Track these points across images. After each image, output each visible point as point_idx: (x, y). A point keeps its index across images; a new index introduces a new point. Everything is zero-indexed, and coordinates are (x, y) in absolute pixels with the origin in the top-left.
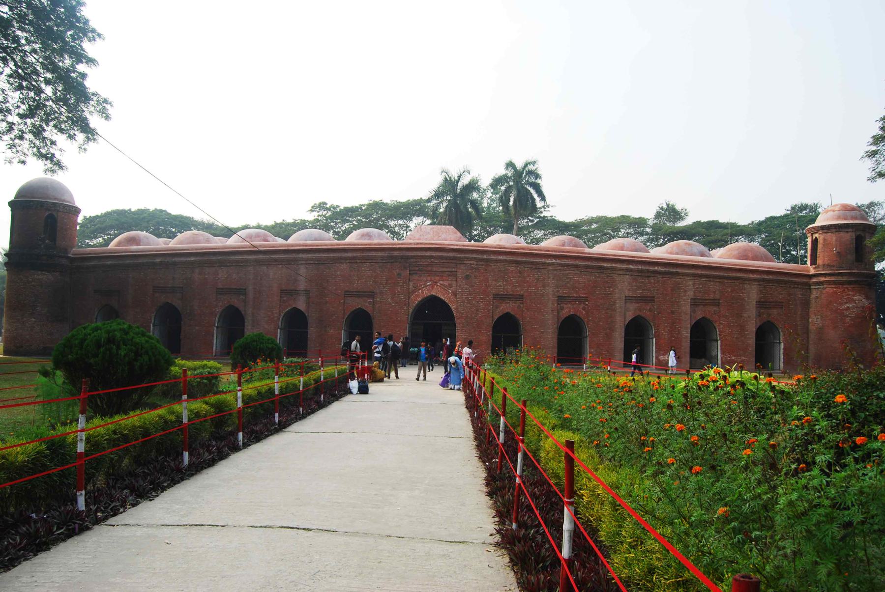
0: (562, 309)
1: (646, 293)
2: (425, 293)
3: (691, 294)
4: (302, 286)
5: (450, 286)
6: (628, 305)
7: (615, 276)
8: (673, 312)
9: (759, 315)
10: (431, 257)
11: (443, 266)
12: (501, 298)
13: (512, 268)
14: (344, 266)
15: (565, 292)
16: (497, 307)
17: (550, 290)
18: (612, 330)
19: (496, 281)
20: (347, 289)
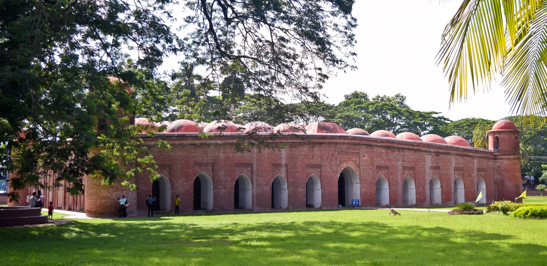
0: (404, 173)
1: (437, 165)
2: (344, 165)
3: (453, 164)
4: (284, 162)
5: (356, 161)
6: (430, 171)
7: (425, 155)
8: (447, 175)
9: (477, 175)
10: (348, 144)
11: (353, 149)
12: (379, 168)
13: (383, 151)
14: (306, 148)
15: (406, 164)
16: (377, 173)
17: (400, 163)
18: (425, 184)
19: (377, 158)
20: (307, 163)
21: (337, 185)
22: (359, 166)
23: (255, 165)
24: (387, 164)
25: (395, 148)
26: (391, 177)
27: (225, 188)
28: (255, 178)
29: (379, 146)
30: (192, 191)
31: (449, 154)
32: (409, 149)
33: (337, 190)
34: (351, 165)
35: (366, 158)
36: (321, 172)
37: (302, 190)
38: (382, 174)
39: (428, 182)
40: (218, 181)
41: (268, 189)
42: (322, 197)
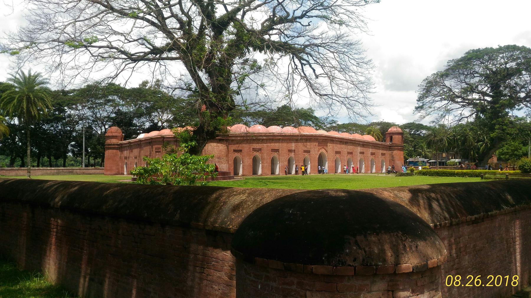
24: (340, 150)
34: (323, 151)
38: (338, 156)
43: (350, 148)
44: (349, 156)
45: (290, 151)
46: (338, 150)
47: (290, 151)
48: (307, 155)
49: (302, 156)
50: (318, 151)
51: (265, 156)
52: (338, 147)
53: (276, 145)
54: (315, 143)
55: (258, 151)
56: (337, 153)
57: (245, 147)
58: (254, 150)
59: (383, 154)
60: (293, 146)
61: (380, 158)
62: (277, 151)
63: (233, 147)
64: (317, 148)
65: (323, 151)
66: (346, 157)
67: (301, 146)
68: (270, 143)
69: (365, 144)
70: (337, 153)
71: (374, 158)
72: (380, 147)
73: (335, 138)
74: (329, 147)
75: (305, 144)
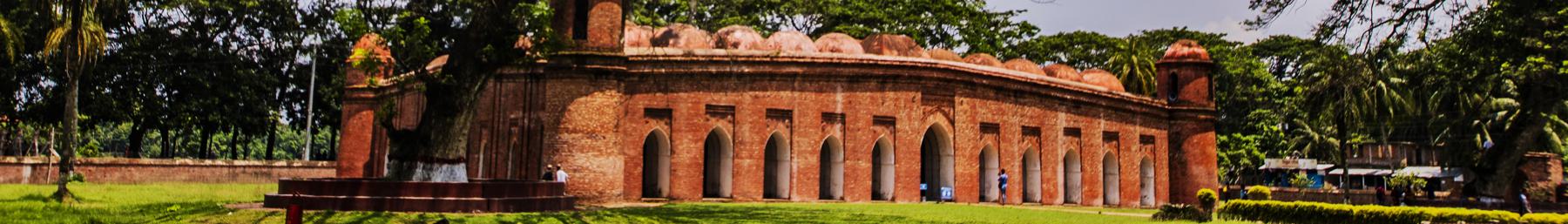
21: (919, 157)
22: (952, 122)
23: (796, 112)
25: (1009, 90)
26: (1002, 145)
27: (751, 157)
28: (796, 138)
29: (984, 86)
30: (701, 161)
31: (1093, 105)
32: (1032, 94)
33: (918, 167)
34: (939, 119)
35: (965, 106)
36: (894, 132)
37: (865, 165)
38: (989, 139)
39: (1060, 158)
40: (741, 143)
41: (814, 160)
42: (897, 180)
43: (1030, 114)
44: (1030, 142)
45: (829, 117)
46: (989, 118)
47: (829, 117)
48: (883, 133)
49: (865, 136)
50: (924, 120)
51: (748, 136)
52: (988, 110)
53: (783, 98)
54: (912, 94)
55: (723, 116)
56: (987, 128)
57: (686, 102)
58: (712, 110)
59: (1146, 140)
60: (838, 100)
61: (1136, 153)
62: (784, 115)
63: (642, 101)
64: (918, 111)
65: (939, 119)
66: (1016, 146)
67: (869, 102)
68: (778, 89)
69: (1083, 103)
70: (987, 128)
71: (1114, 151)
72: (1134, 113)
73: (980, 75)
74: (958, 108)
75: (878, 95)
